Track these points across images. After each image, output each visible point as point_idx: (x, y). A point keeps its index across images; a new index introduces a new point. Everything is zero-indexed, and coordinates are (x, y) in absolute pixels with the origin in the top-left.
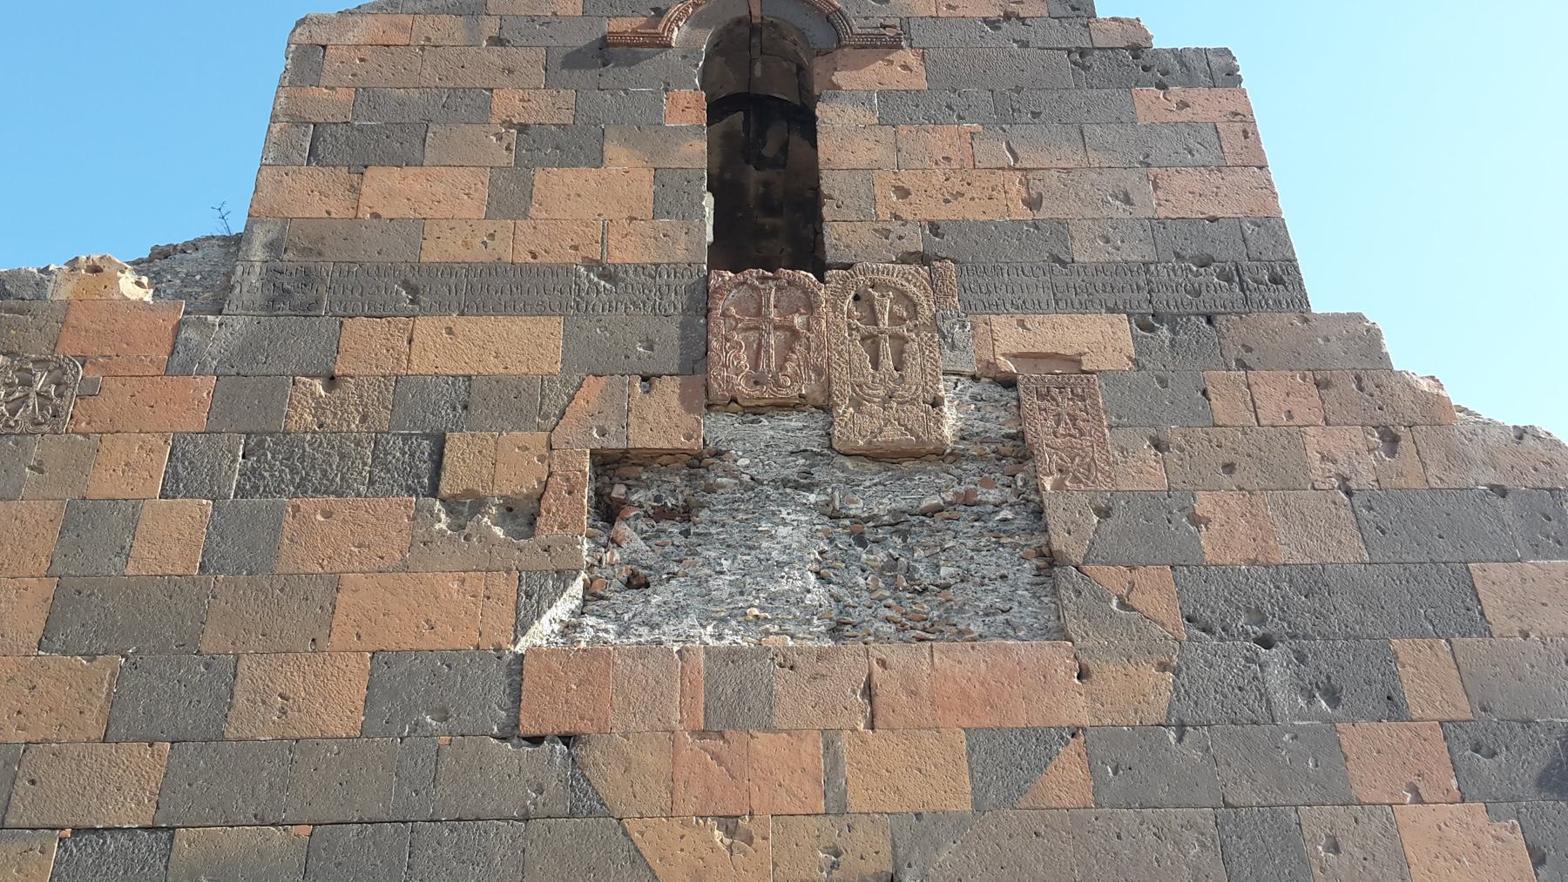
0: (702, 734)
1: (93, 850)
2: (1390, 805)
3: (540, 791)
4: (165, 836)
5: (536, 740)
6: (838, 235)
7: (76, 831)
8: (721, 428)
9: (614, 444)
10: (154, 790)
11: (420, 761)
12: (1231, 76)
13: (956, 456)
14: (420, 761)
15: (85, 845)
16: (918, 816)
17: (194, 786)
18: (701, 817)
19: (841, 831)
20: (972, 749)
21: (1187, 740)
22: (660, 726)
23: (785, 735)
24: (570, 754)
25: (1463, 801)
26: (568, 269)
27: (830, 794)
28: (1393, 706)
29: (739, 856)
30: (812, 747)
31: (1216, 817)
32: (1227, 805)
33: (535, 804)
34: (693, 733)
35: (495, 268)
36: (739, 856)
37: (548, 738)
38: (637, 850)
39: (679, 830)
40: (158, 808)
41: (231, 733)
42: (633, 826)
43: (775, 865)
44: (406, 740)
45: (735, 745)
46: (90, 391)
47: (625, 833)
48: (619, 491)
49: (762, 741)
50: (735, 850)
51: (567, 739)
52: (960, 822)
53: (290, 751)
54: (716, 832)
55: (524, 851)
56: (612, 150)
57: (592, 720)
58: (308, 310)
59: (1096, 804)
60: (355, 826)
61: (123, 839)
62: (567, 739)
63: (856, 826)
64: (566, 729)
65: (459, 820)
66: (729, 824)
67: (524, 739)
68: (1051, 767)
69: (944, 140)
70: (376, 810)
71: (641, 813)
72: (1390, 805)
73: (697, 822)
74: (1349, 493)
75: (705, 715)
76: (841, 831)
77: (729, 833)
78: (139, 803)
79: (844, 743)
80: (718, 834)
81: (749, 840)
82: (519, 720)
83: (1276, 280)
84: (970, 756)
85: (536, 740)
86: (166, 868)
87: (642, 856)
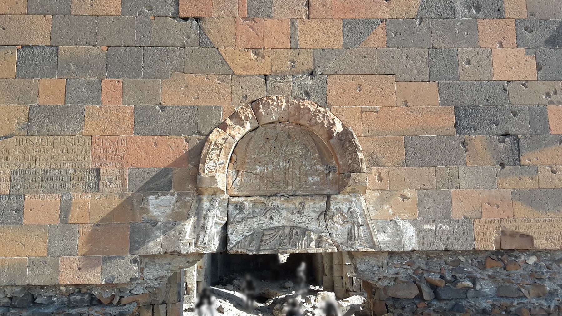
0: (246, 19)
1: (30, 53)
2: (491, 48)
3: (188, 37)
4: (55, 49)
5: (186, 19)
7: (23, 46)
10: (48, 32)
11: (144, 25)
14: (144, 25)
15: (27, 51)
16: (323, 50)
17: (63, 31)
18: (246, 49)
19: (296, 54)
20: (344, 26)
21: (422, 24)
22: (231, 15)
23: (277, 20)
24: (198, 24)
25: (517, 47)
27: (292, 42)
28: (499, 13)
29: (259, 63)
30: (286, 25)
31: (429, 52)
32: (433, 47)
33: (187, 42)
34: (243, 18)
36: (259, 63)
37: (190, 18)
38: (224, 59)
39: (239, 53)
40: (51, 39)
41: (73, 12)
42: (222, 51)
43: (272, 66)
44: (138, 17)
45: (258, 23)
47: (219, 53)
49: (268, 22)
50: (258, 61)
51: (197, 19)
52: (338, 53)
53: (96, 20)
54: (252, 54)
55: (184, 58)
57: (206, 12)
59: (387, 46)
60: (123, 47)
61: (40, 49)
62: (197, 19)
63: (301, 53)
64: (196, 15)
65: (160, 46)
66: (256, 51)
67: (182, 18)
68: (372, 33)
70: (130, 42)
71: (225, 47)
72: (491, 48)
73: (245, 50)
75: (247, 12)
76: (296, 54)
77: (256, 54)
78: (44, 37)
79: (298, 23)
80: (252, 55)
81: (263, 57)
82: (179, 11)
84: (343, 29)
85: (186, 19)
86: (57, 60)
87: (225, 61)
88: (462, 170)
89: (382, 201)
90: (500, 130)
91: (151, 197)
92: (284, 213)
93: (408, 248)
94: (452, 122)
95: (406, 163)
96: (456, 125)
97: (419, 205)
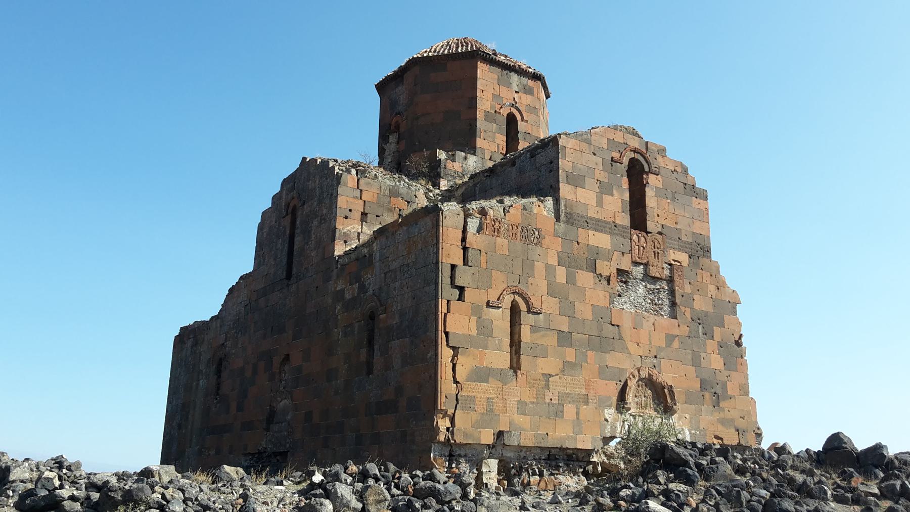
5: (613, 325)
12: (706, 198)
16: (659, 347)
28: (712, 338)
74: (712, 298)
83: (708, 251)
90: (713, 391)
91: (606, 410)
94: (699, 386)
95: (686, 403)
96: (701, 387)
97: (690, 422)
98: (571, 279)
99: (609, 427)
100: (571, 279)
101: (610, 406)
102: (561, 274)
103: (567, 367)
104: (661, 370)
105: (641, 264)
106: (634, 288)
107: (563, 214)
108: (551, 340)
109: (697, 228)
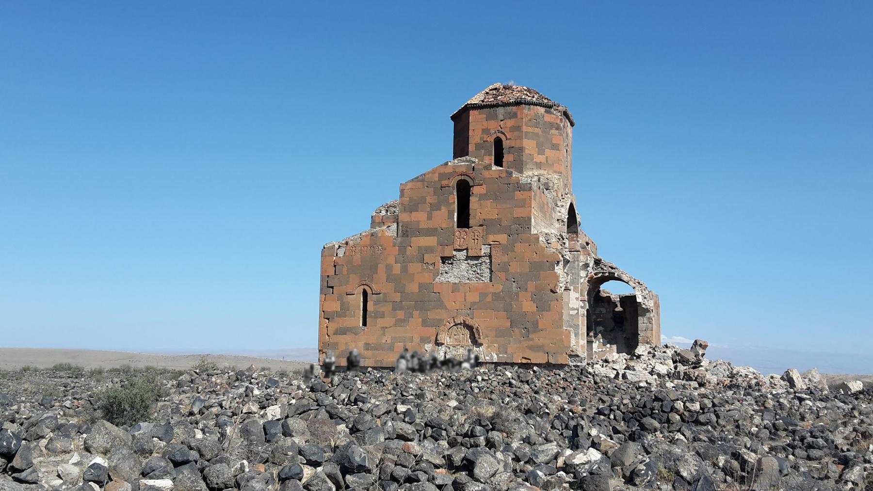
6: (471, 222)
8: (454, 253)
9: (443, 256)
13: (483, 256)
26: (437, 229)
35: (428, 229)
46: (385, 249)
48: (444, 261)
51: (439, 293)
56: (443, 207)
58: (407, 236)
69: (488, 203)
88: (511, 339)
89: (488, 347)
92: (461, 350)
93: (495, 361)
98: (405, 269)
99: (428, 355)
100: (405, 269)
101: (429, 342)
102: (397, 269)
103: (400, 322)
104: (473, 316)
105: (464, 250)
106: (457, 267)
107: (400, 232)
108: (387, 308)
109: (519, 213)
